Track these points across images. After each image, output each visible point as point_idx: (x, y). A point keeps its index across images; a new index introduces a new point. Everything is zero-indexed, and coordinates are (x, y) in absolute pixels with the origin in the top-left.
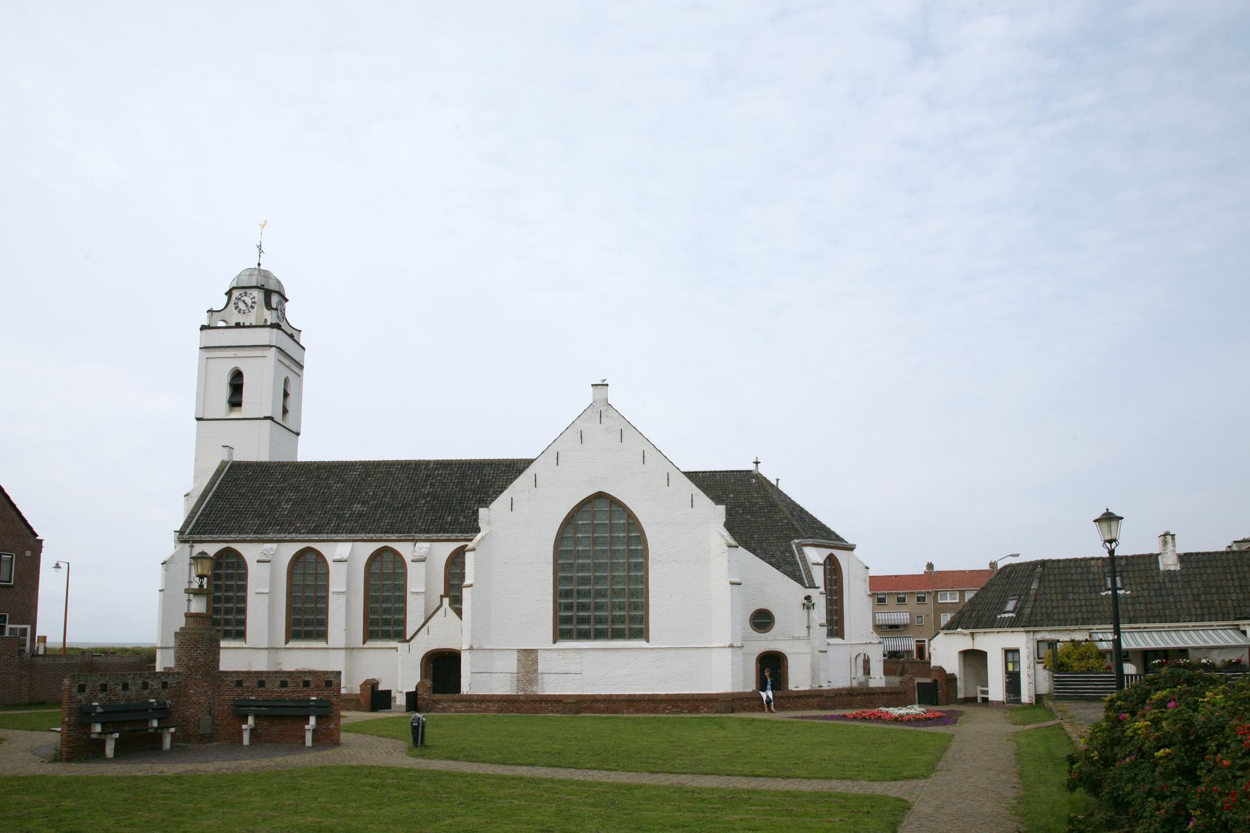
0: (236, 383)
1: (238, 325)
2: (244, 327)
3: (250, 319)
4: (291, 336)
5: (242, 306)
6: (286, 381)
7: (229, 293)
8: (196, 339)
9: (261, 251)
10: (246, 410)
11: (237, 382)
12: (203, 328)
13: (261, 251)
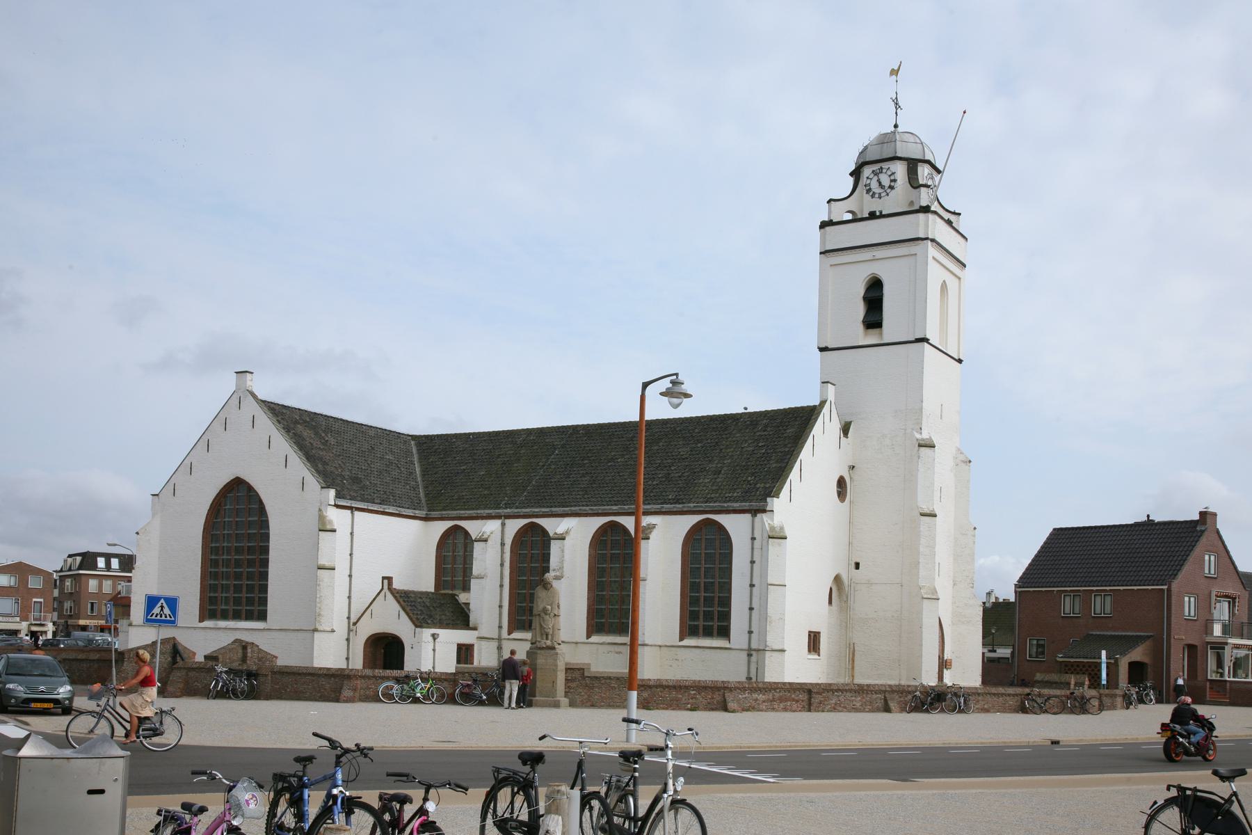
1: (873, 216)
2: (882, 216)
3: (887, 205)
4: (949, 222)
6: (944, 286)
7: (856, 174)
8: (814, 240)
11: (873, 294)
12: (824, 225)
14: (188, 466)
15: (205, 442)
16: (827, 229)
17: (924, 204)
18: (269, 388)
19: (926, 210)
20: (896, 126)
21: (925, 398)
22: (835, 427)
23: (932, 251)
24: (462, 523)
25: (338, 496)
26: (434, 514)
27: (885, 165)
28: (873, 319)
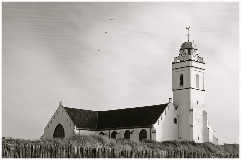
0: (182, 78)
5: (183, 55)
7: (180, 51)
9: (188, 35)
10: (185, 86)
12: (173, 63)
13: (188, 35)
14: (51, 122)
15: (54, 117)
16: (173, 64)
17: (190, 59)
18: (65, 105)
19: (190, 60)
20: (188, 40)
21: (191, 100)
22: (173, 107)
23: (191, 68)
24: (103, 131)
25: (76, 127)
26: (98, 129)
27: (184, 50)
28: (182, 84)
